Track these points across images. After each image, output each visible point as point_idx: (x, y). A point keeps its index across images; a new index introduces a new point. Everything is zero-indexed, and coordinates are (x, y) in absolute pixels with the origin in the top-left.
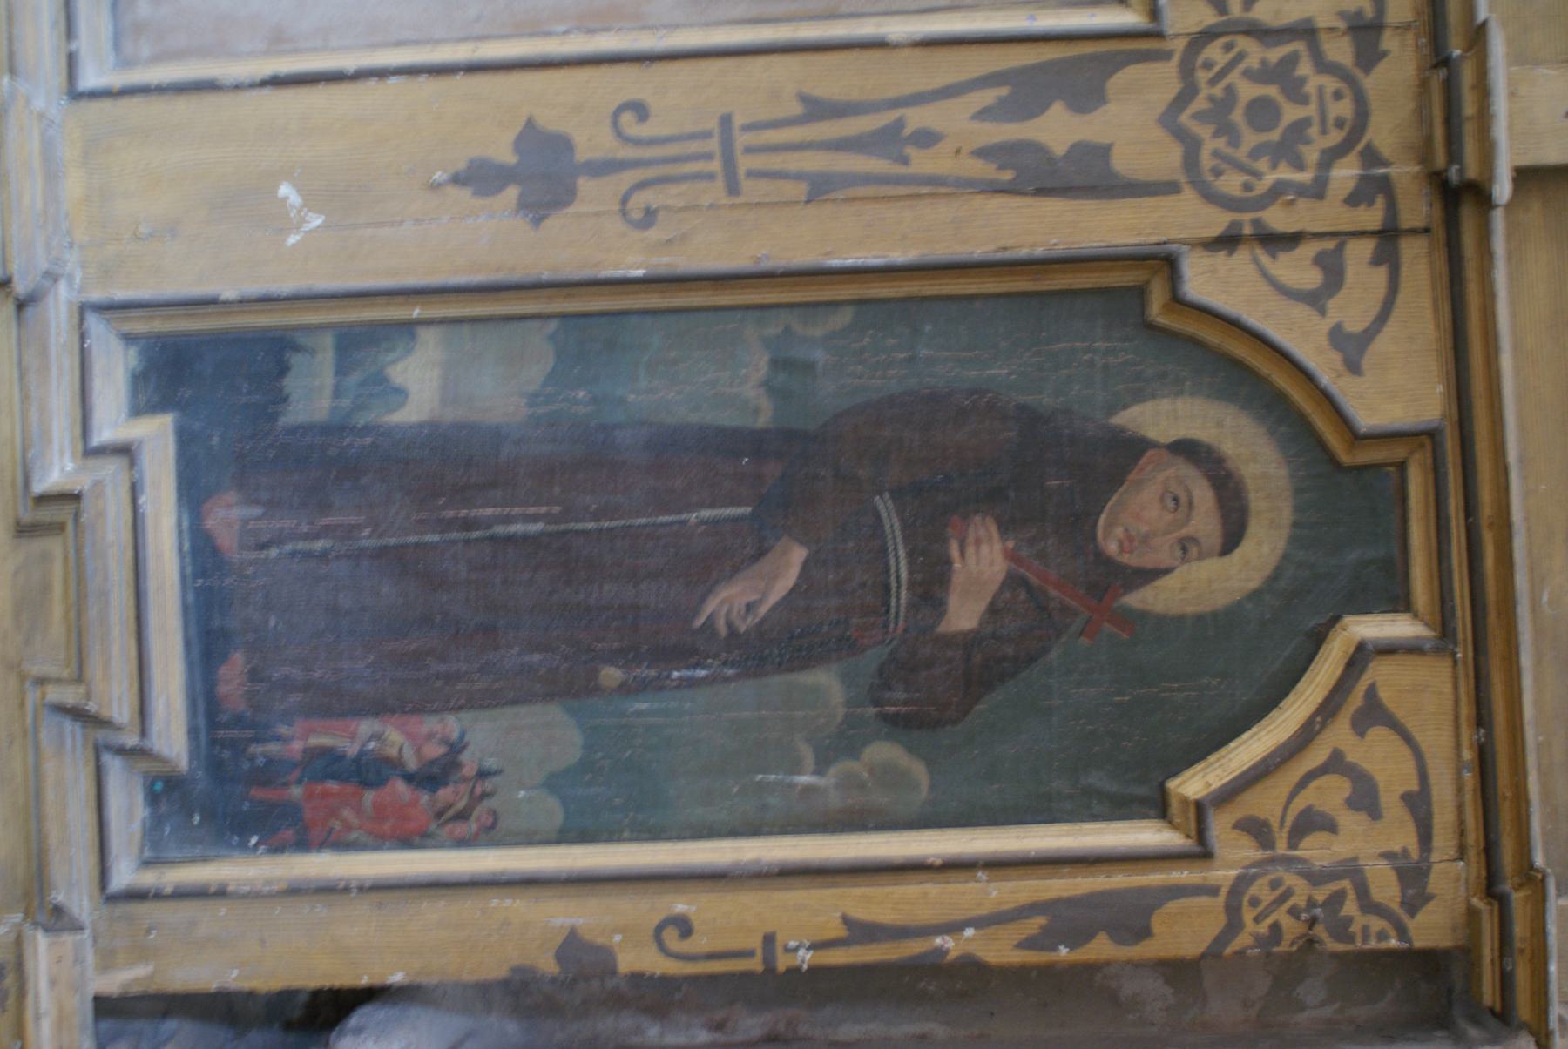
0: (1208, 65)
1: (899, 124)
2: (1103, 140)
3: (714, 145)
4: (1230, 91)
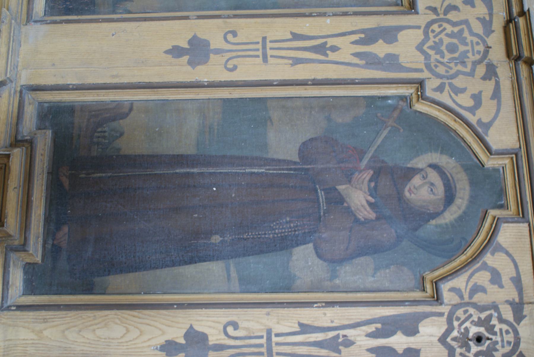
0: (433, 31)
1: (326, 43)
2: (397, 53)
3: (260, 46)
4: (441, 40)
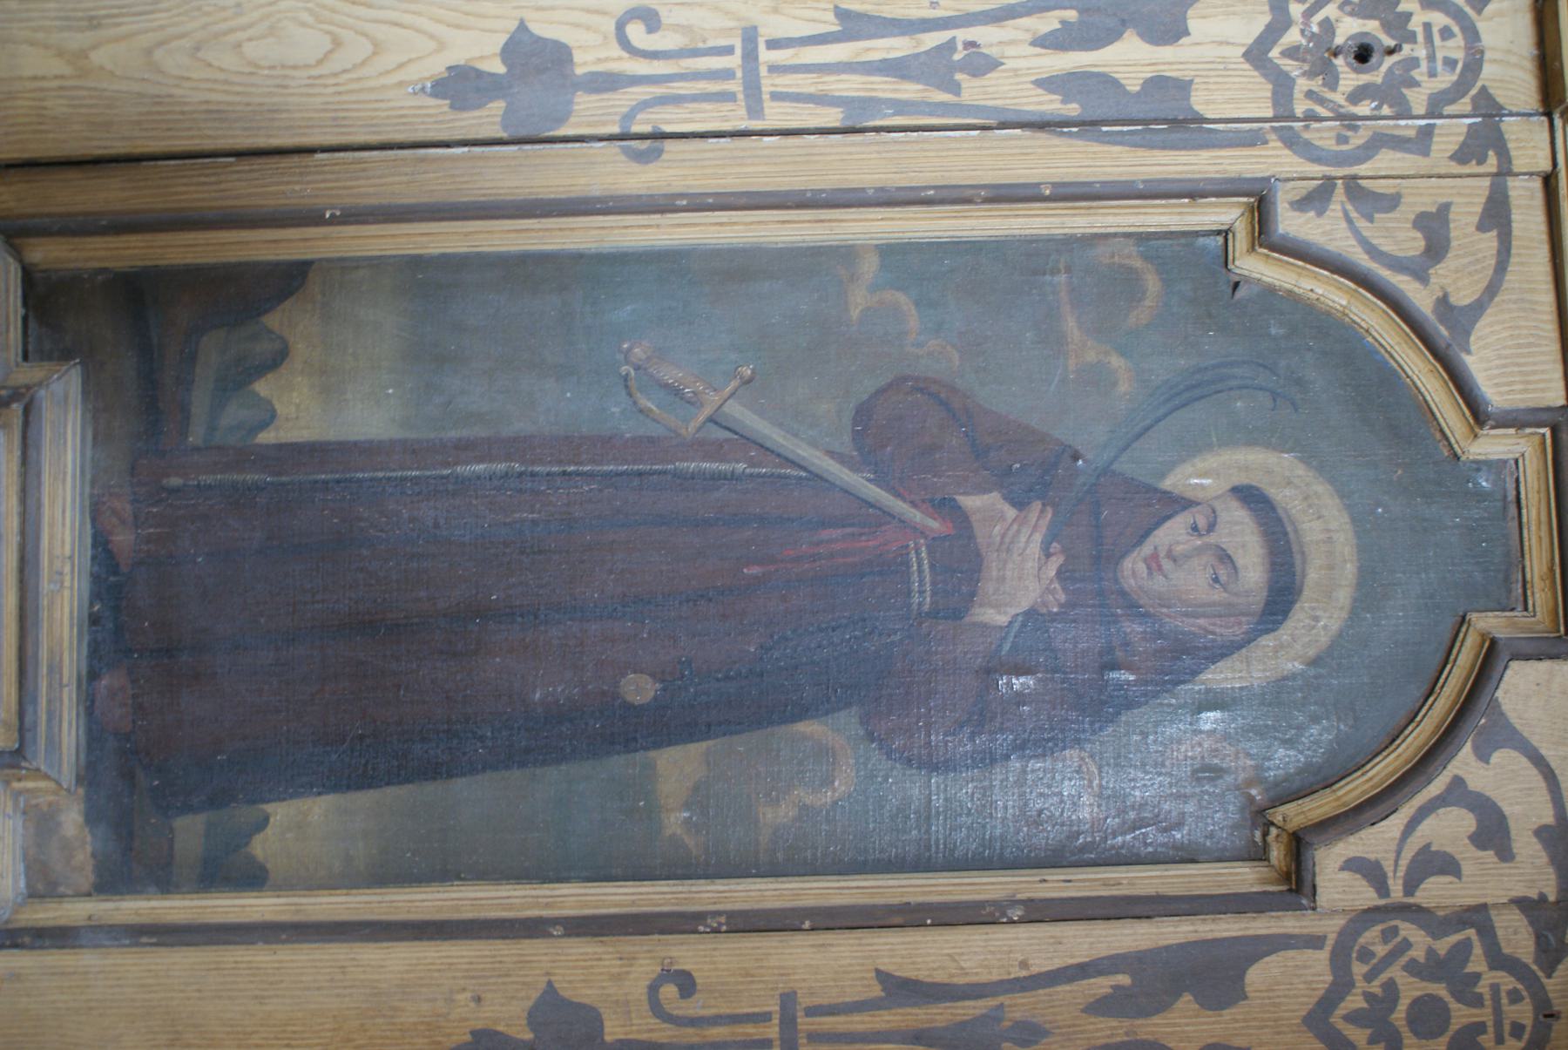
3: (734, 61)
